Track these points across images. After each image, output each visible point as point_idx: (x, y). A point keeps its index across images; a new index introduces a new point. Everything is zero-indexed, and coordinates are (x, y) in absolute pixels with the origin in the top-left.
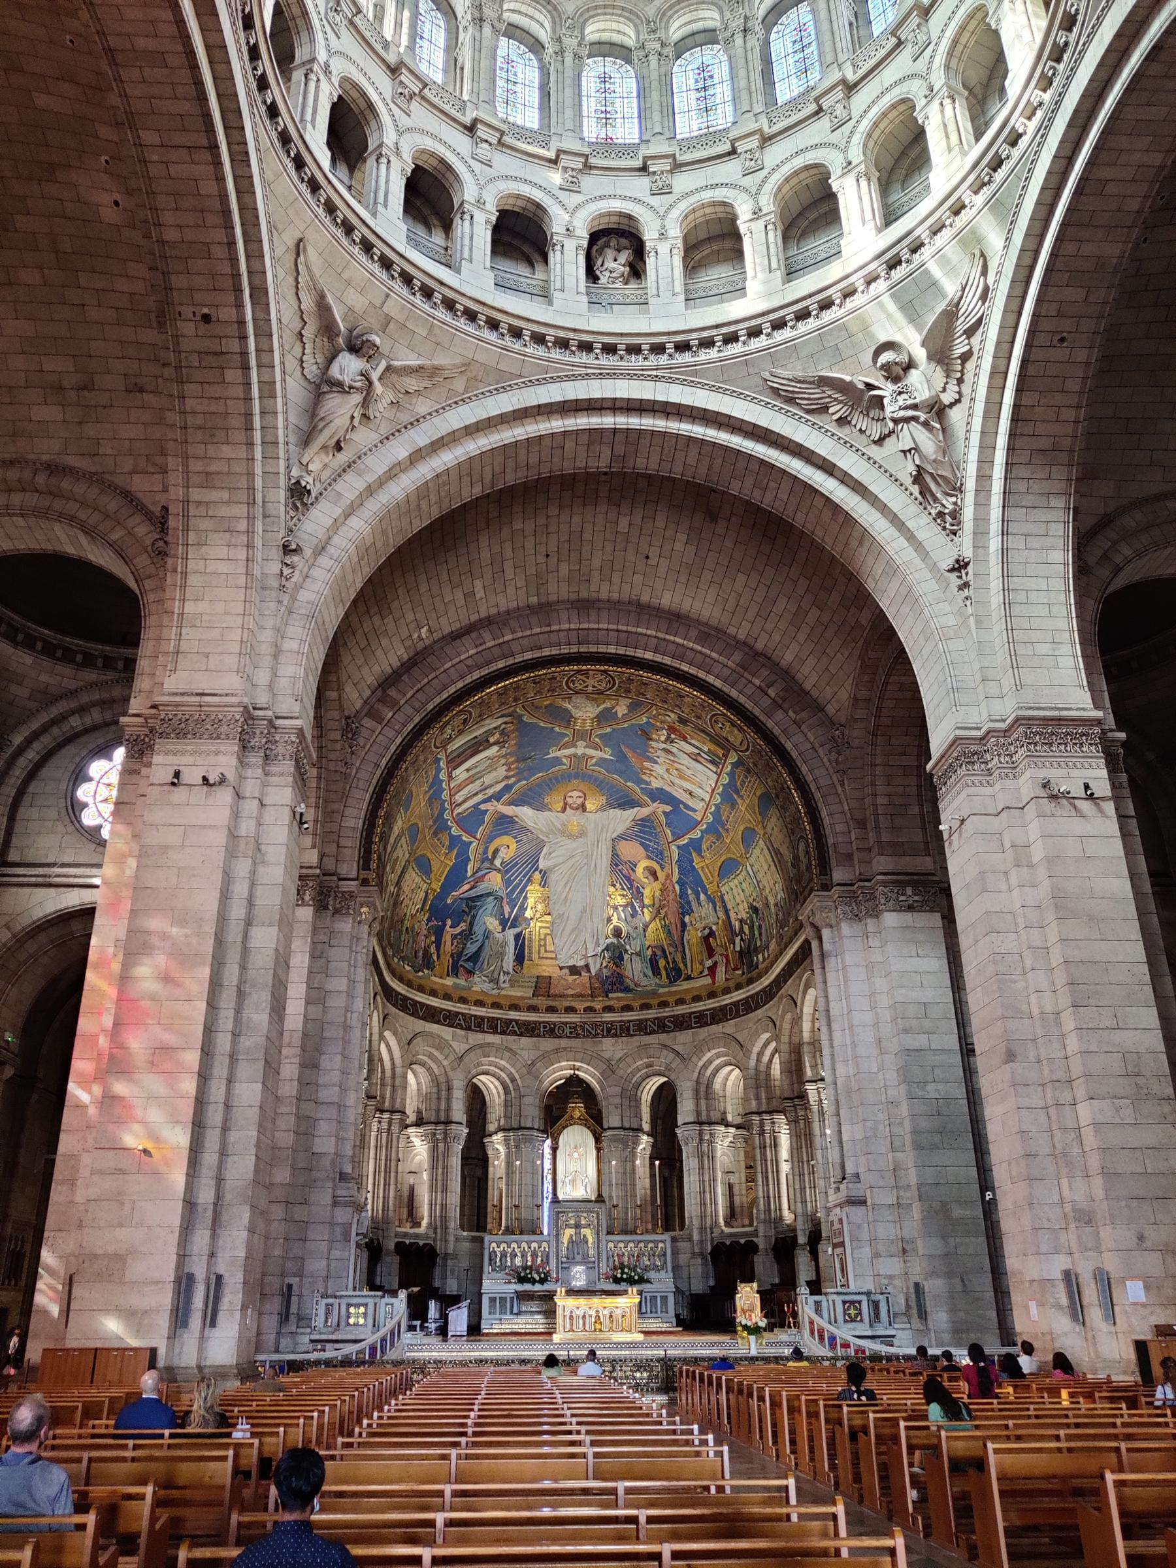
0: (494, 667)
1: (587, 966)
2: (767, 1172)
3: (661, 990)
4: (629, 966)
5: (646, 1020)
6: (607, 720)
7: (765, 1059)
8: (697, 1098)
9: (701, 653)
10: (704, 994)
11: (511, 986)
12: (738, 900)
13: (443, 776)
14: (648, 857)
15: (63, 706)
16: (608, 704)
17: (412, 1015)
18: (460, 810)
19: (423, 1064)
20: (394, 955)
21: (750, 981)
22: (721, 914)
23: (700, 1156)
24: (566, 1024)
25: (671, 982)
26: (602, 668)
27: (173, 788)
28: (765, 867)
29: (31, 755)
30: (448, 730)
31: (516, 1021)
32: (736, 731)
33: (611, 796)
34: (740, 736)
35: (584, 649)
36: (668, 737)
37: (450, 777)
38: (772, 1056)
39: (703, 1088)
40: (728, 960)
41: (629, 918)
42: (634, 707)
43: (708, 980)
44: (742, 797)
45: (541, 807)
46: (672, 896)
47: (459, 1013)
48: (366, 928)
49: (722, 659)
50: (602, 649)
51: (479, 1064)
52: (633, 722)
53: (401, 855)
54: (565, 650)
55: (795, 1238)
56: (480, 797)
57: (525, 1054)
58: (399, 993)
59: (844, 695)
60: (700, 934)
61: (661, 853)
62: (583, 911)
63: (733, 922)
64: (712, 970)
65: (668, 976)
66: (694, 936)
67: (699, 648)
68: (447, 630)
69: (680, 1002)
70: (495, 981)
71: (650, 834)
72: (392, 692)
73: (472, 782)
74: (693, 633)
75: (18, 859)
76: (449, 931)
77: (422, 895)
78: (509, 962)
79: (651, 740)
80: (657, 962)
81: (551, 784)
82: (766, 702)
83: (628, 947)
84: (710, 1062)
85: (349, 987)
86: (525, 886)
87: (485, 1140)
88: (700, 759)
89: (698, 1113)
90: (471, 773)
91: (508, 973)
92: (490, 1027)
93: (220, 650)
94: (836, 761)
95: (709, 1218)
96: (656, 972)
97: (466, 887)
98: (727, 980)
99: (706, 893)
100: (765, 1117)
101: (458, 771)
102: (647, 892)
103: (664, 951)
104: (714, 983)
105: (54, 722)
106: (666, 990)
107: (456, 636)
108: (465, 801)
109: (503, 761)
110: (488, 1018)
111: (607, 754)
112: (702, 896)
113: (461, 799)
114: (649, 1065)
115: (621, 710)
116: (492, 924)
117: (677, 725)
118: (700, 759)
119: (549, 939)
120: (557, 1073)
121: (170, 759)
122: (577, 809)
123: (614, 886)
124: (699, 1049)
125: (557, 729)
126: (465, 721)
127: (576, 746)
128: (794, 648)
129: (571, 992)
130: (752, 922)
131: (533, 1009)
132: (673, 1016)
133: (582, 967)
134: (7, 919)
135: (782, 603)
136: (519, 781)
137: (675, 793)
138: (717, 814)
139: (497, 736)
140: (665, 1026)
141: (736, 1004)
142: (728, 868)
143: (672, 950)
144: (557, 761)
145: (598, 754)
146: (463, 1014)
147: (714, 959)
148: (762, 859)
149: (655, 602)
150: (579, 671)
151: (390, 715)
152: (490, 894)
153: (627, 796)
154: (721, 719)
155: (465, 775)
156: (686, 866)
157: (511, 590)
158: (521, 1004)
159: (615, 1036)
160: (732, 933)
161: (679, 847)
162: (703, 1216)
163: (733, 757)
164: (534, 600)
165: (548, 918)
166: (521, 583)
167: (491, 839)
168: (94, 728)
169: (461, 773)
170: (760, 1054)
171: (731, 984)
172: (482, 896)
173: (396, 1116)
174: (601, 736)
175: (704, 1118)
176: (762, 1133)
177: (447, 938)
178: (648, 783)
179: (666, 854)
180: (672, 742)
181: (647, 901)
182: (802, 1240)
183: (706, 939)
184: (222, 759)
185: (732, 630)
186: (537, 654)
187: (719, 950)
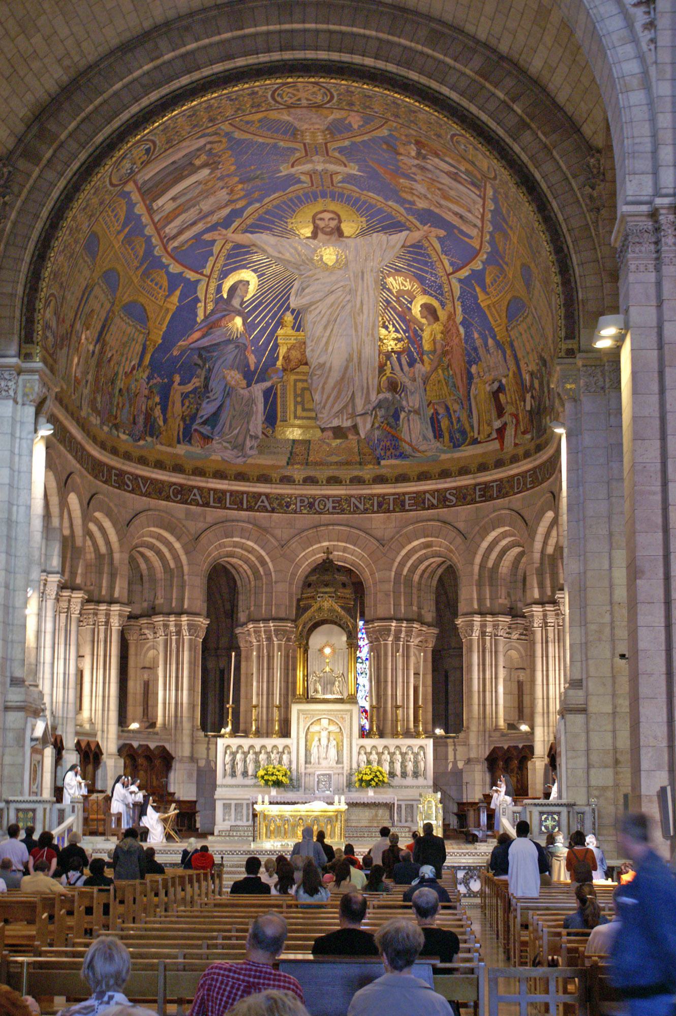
0: (176, 84)
1: (355, 427)
3: (443, 457)
4: (406, 426)
5: (425, 492)
6: (340, 132)
9: (432, 57)
10: (491, 462)
11: (261, 452)
13: (140, 209)
14: (425, 292)
16: (337, 115)
17: (132, 491)
18: (176, 244)
19: (151, 547)
20: (103, 423)
22: (513, 367)
24: (328, 497)
26: (313, 80)
30: (127, 164)
31: (267, 495)
32: (480, 157)
33: (372, 216)
35: (288, 55)
36: (419, 153)
37: (150, 210)
40: (517, 420)
41: (406, 368)
42: (367, 120)
43: (496, 445)
45: (287, 233)
46: (456, 341)
47: (193, 487)
48: (31, 410)
49: (458, 66)
50: (310, 55)
51: (221, 546)
52: (374, 134)
53: (96, 306)
54: (263, 58)
55: (531, 749)
56: (200, 227)
57: (278, 532)
58: (110, 468)
60: (488, 388)
61: (440, 287)
62: (349, 360)
63: (523, 372)
64: (501, 431)
65: (451, 438)
66: (481, 390)
67: (430, 52)
68: (115, 42)
69: (464, 471)
70: (239, 447)
71: (426, 264)
72: (51, 126)
73: (186, 211)
74: (423, 33)
76: (178, 390)
77: (139, 348)
78: (257, 422)
79: (401, 154)
80: (439, 422)
81: (292, 206)
82: (511, 121)
83: (404, 403)
85: (12, 477)
86: (274, 330)
87: (238, 630)
90: (179, 202)
91: (256, 437)
92: (234, 503)
94: (591, 197)
96: (438, 434)
97: (197, 335)
98: (516, 445)
99: (494, 337)
101: (160, 202)
102: (426, 335)
103: (447, 409)
104: (502, 449)
106: (448, 456)
107: (126, 48)
108: (180, 233)
109: (221, 184)
110: (232, 493)
111: (353, 169)
112: (490, 342)
113: (175, 232)
114: (427, 546)
115: (355, 121)
116: (234, 377)
117: (423, 140)
118: (459, 179)
119: (307, 395)
120: (312, 555)
122: (330, 233)
123: (386, 328)
125: (281, 144)
126: (148, 151)
127: (311, 162)
129: (335, 459)
131: (287, 480)
132: (455, 488)
133: (349, 428)
136: (250, 204)
137: (444, 215)
138: (492, 242)
139: (204, 158)
140: (445, 499)
141: (523, 475)
143: (456, 407)
144: (292, 180)
145: (346, 170)
146: (199, 488)
147: (503, 419)
150: (283, 84)
151: (51, 152)
152: (229, 341)
153: (389, 216)
154: (460, 138)
155: (171, 206)
158: (275, 475)
159: (388, 511)
160: (523, 389)
161: (460, 281)
165: (303, 368)
167: (225, 275)
169: (164, 203)
171: (520, 451)
172: (218, 344)
173: (115, 608)
174: (341, 150)
177: (176, 396)
178: (411, 203)
180: (424, 158)
181: (427, 346)
183: (495, 394)
185: (470, 28)
186: (229, 65)
187: (509, 409)
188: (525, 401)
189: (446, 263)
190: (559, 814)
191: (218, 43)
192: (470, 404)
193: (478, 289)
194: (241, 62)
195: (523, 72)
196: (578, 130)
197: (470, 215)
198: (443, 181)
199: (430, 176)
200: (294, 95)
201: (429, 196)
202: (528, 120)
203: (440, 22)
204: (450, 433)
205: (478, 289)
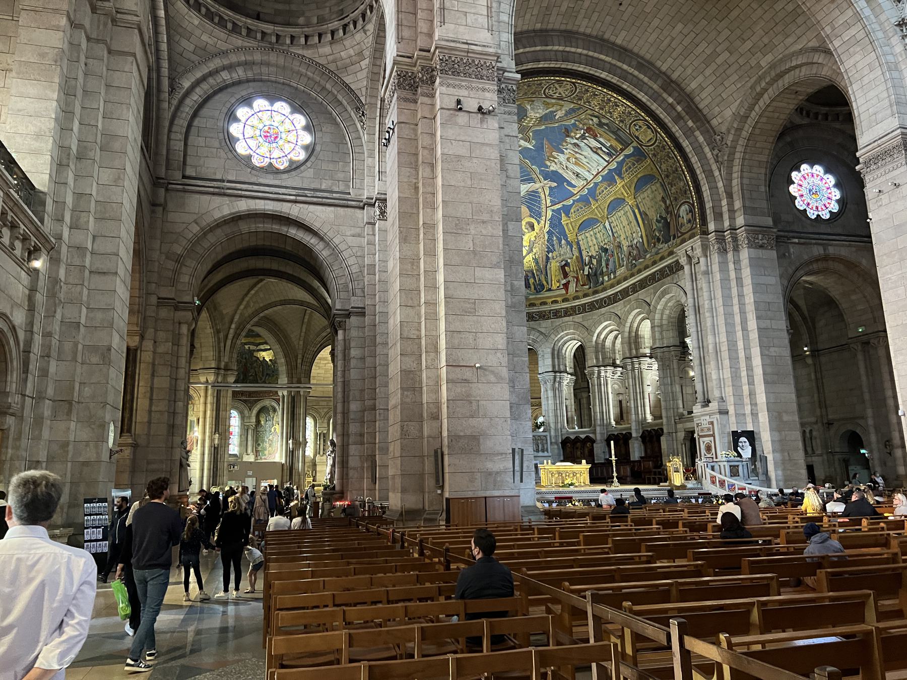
2: (602, 399)
3: (531, 297)
7: (602, 337)
8: (553, 358)
12: (591, 244)
14: (531, 216)
15: (216, 63)
21: (596, 292)
22: (576, 253)
23: (554, 389)
25: (537, 292)
27: (457, 113)
28: (625, 223)
29: (196, 97)
34: (650, 134)
38: (608, 335)
39: (556, 353)
43: (564, 291)
44: (622, 178)
59: (728, 113)
64: (566, 286)
65: (535, 289)
66: (554, 265)
67: (636, 73)
74: (634, 63)
75: (194, 174)
79: (568, 136)
80: (528, 280)
82: (674, 114)
84: (562, 338)
88: (600, 152)
89: (554, 366)
93: (473, 11)
95: (559, 424)
99: (566, 240)
100: (602, 368)
103: (533, 274)
104: (567, 293)
105: (211, 74)
106: (534, 296)
112: (563, 242)
118: (600, 152)
121: (451, 90)
124: (556, 330)
128: (700, 79)
130: (601, 257)
132: (538, 312)
134: (195, 217)
135: (704, 45)
137: (565, 175)
140: (533, 317)
142: (585, 225)
147: (567, 279)
148: (624, 219)
149: (612, 39)
156: (555, 223)
157: (528, 16)
161: (553, 211)
162: (556, 423)
163: (629, 151)
164: (538, 26)
166: (535, 12)
168: (239, 83)
170: (600, 333)
171: (580, 294)
174: (535, 132)
175: (557, 369)
176: (599, 377)
179: (544, 214)
182: (634, 435)
183: (563, 268)
184: (487, 95)
185: (659, 64)
187: (572, 274)
188: (583, 271)
189: (548, 201)
190: (738, 466)
191: (533, 51)
192: (547, 272)
193: (563, 215)
194: (541, 65)
195: (683, 90)
196: (708, 122)
197: (587, 173)
198: (583, 153)
199: (577, 150)
200: (556, 89)
201: (564, 163)
202: (684, 114)
203: (642, 58)
204: (534, 285)
205: (563, 215)
